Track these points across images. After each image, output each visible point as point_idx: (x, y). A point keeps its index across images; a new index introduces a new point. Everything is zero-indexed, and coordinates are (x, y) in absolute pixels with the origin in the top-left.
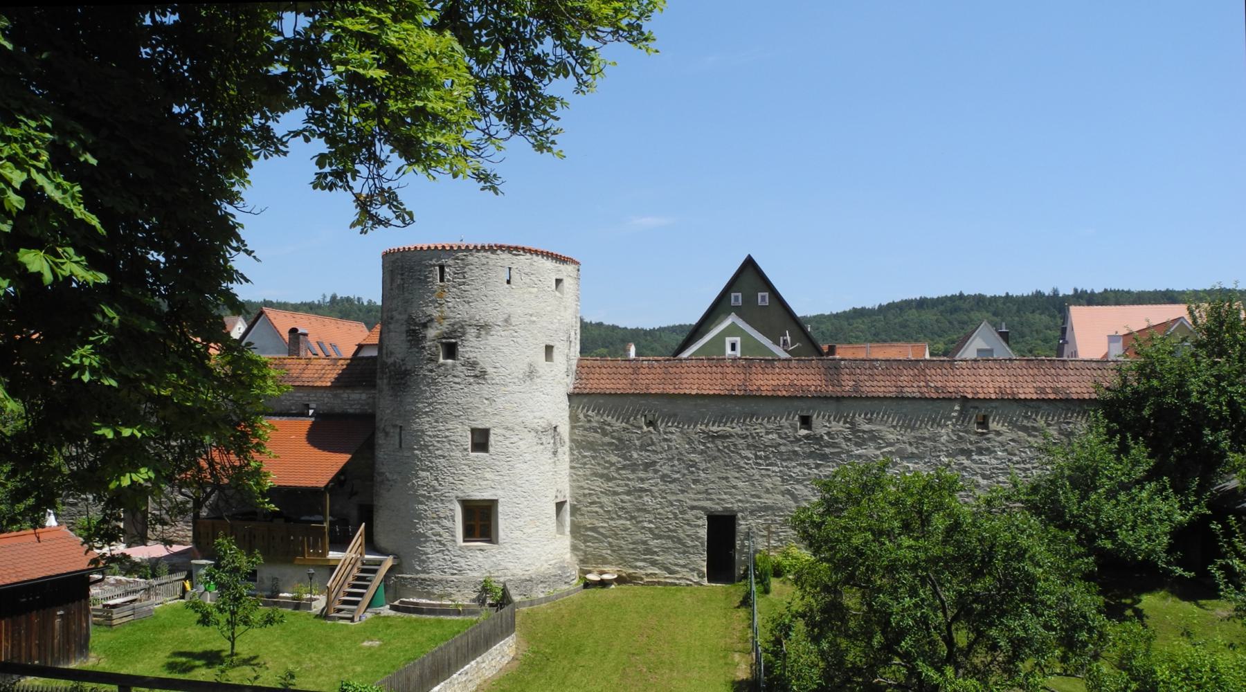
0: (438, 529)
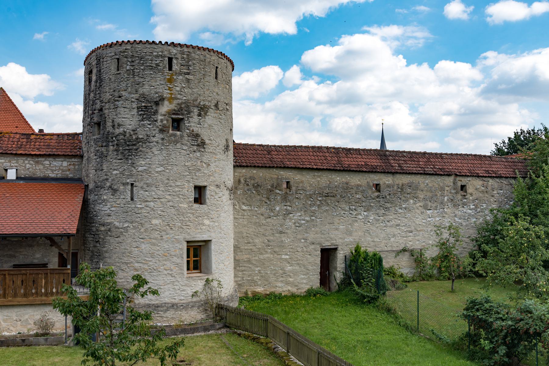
0: (168, 264)
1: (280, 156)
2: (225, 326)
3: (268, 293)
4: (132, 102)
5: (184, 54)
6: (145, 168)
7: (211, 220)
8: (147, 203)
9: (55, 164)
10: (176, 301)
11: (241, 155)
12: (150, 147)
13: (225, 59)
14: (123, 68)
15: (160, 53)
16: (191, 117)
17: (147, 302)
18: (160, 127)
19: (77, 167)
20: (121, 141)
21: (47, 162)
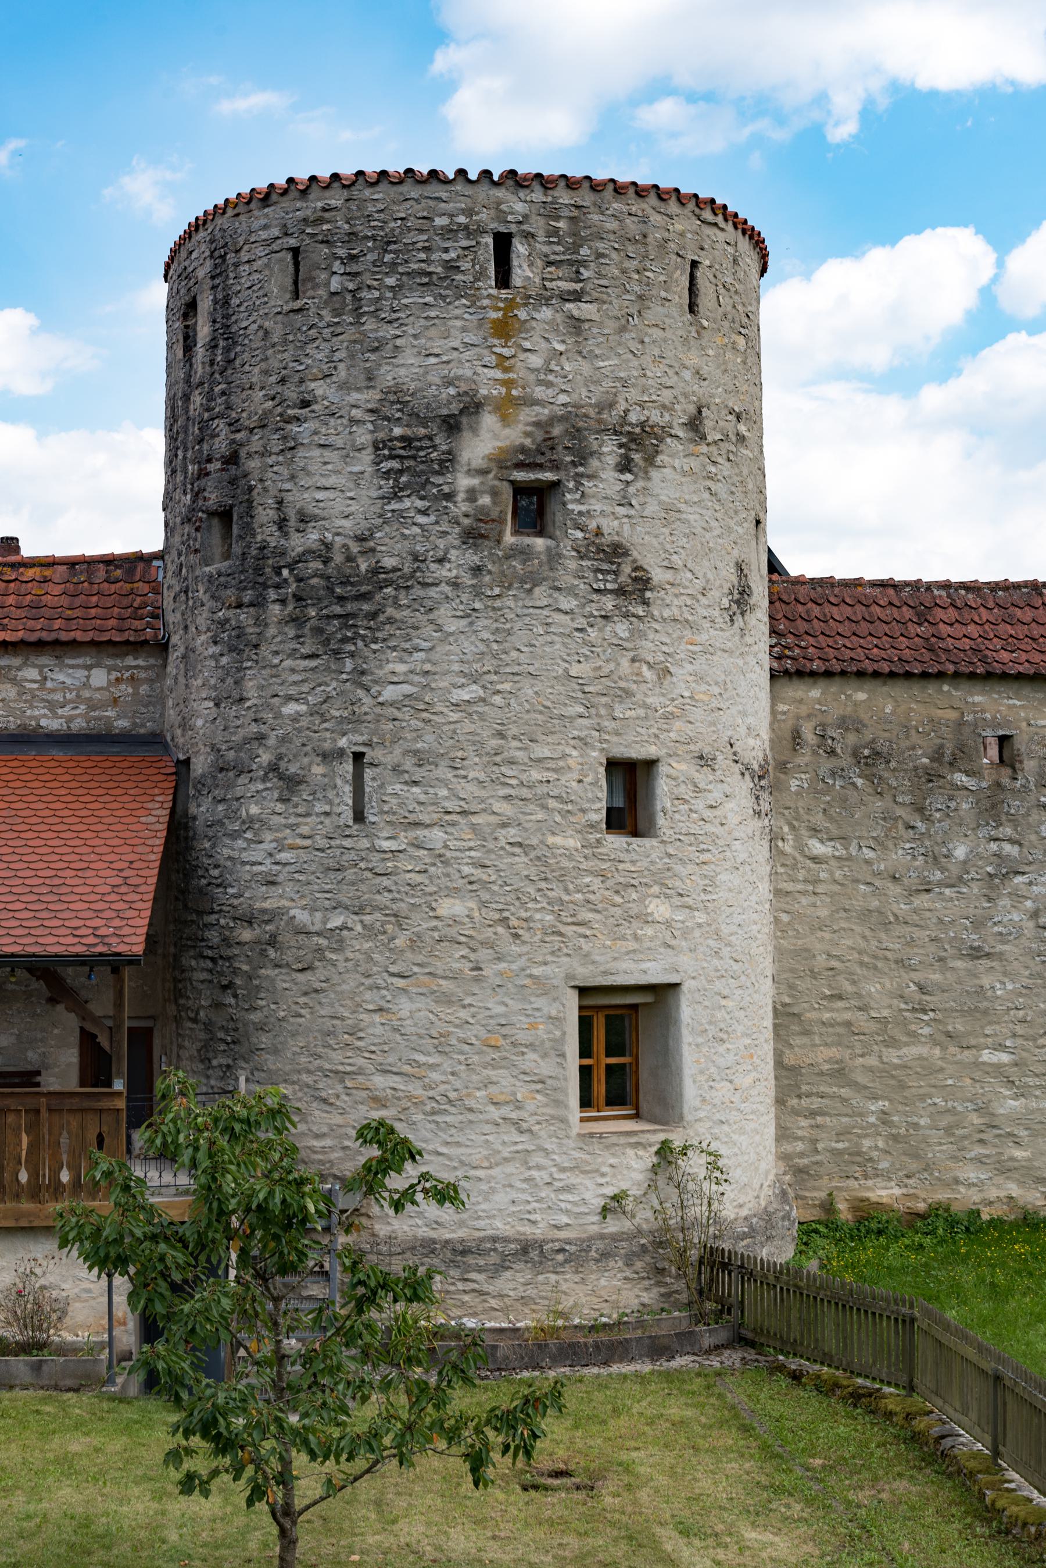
0: (505, 1081)
1: (972, 630)
2: (740, 1340)
3: (921, 1207)
4: (353, 421)
5: (557, 218)
6: (407, 689)
7: (677, 901)
8: (420, 833)
9: (61, 677)
10: (537, 1233)
11: (802, 626)
12: (429, 603)
13: (730, 227)
14: (316, 287)
15: (462, 219)
16: (590, 477)
17: (424, 1232)
18: (466, 521)
19: (144, 689)
20: (314, 581)
21: (32, 673)
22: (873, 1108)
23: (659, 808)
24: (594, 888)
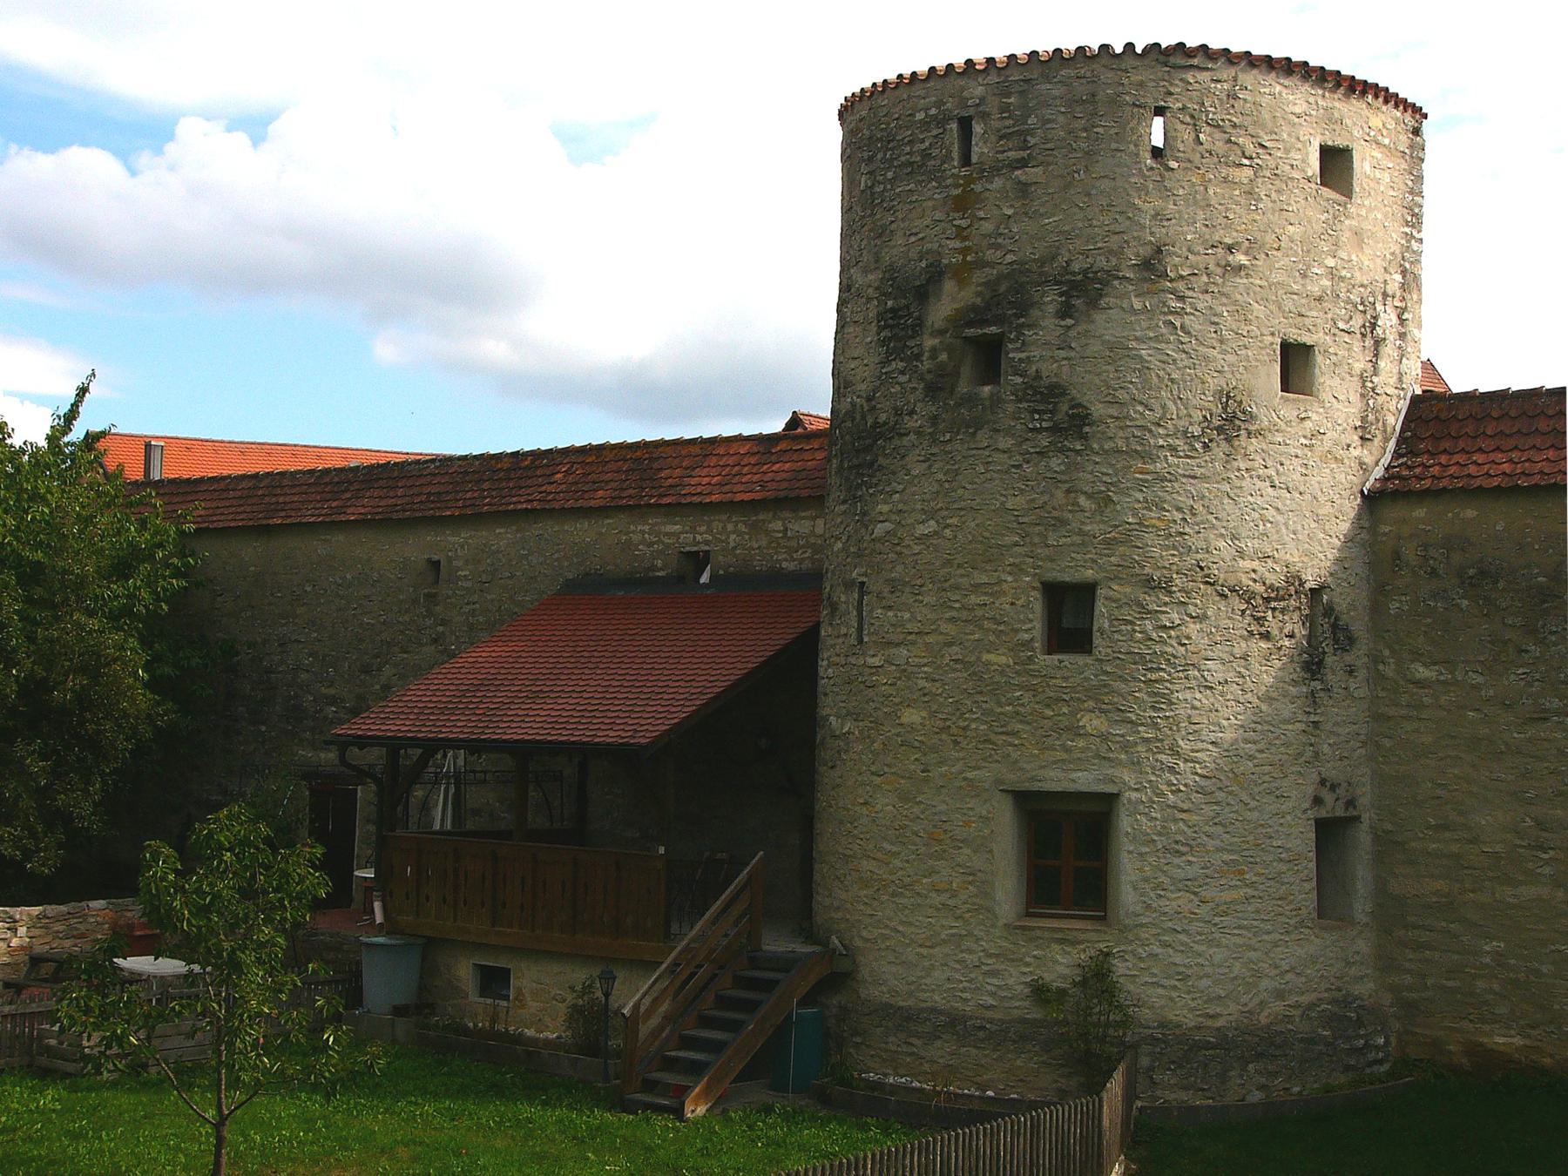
5: (1008, 95)
15: (933, 111)
16: (1030, 327)
21: (778, 525)
22: (1487, 948)
23: (1095, 628)
24: (1025, 701)
